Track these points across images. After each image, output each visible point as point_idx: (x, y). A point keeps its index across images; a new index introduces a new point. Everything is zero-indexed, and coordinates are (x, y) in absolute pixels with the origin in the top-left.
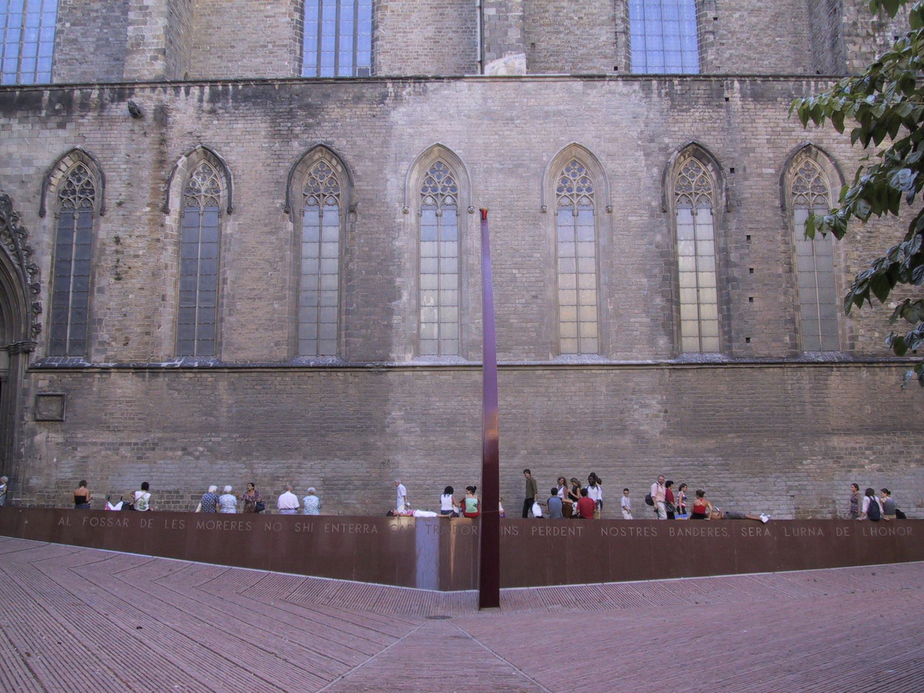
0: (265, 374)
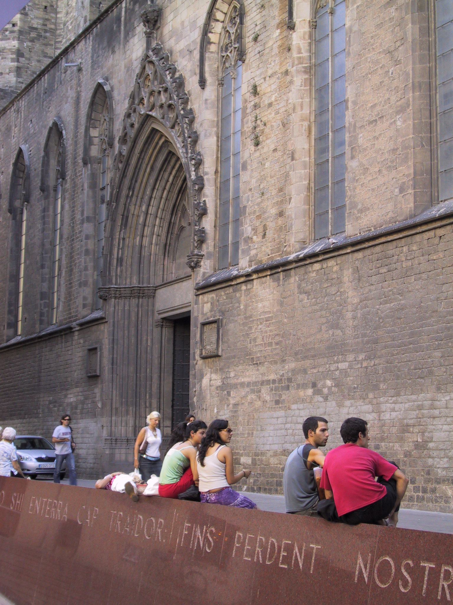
0: (390, 246)
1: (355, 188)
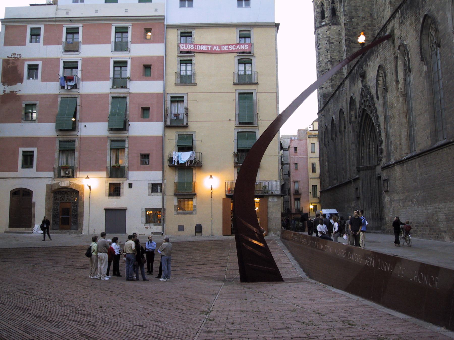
1: (417, 137)
